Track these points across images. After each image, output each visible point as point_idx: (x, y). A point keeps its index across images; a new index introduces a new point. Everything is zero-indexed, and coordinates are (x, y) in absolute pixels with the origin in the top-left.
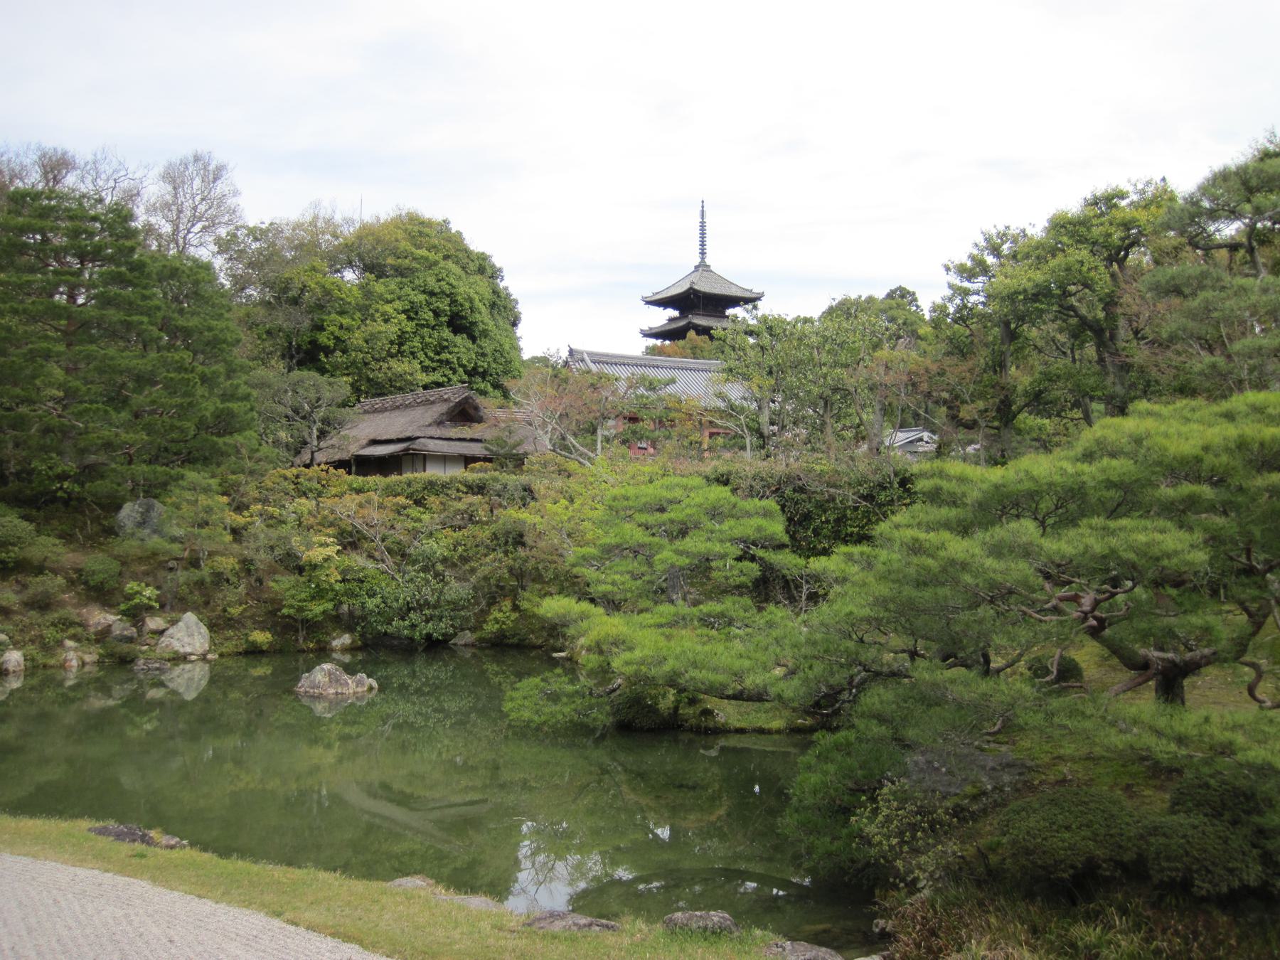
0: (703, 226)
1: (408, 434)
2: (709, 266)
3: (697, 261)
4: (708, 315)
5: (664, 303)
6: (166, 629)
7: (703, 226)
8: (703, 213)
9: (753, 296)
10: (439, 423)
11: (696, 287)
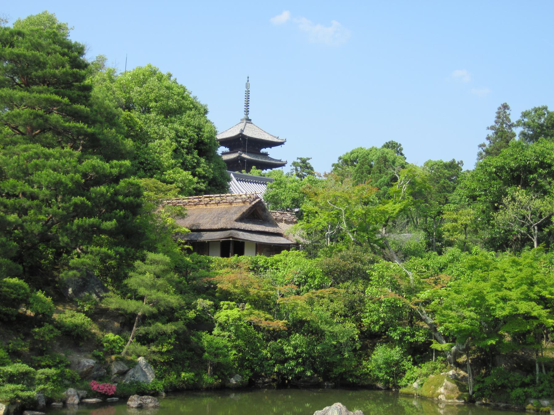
0: (248, 93)
2: (250, 120)
3: (243, 116)
4: (249, 153)
6: (128, 371)
7: (248, 93)
8: (247, 86)
9: (279, 141)
10: (242, 219)
11: (244, 133)
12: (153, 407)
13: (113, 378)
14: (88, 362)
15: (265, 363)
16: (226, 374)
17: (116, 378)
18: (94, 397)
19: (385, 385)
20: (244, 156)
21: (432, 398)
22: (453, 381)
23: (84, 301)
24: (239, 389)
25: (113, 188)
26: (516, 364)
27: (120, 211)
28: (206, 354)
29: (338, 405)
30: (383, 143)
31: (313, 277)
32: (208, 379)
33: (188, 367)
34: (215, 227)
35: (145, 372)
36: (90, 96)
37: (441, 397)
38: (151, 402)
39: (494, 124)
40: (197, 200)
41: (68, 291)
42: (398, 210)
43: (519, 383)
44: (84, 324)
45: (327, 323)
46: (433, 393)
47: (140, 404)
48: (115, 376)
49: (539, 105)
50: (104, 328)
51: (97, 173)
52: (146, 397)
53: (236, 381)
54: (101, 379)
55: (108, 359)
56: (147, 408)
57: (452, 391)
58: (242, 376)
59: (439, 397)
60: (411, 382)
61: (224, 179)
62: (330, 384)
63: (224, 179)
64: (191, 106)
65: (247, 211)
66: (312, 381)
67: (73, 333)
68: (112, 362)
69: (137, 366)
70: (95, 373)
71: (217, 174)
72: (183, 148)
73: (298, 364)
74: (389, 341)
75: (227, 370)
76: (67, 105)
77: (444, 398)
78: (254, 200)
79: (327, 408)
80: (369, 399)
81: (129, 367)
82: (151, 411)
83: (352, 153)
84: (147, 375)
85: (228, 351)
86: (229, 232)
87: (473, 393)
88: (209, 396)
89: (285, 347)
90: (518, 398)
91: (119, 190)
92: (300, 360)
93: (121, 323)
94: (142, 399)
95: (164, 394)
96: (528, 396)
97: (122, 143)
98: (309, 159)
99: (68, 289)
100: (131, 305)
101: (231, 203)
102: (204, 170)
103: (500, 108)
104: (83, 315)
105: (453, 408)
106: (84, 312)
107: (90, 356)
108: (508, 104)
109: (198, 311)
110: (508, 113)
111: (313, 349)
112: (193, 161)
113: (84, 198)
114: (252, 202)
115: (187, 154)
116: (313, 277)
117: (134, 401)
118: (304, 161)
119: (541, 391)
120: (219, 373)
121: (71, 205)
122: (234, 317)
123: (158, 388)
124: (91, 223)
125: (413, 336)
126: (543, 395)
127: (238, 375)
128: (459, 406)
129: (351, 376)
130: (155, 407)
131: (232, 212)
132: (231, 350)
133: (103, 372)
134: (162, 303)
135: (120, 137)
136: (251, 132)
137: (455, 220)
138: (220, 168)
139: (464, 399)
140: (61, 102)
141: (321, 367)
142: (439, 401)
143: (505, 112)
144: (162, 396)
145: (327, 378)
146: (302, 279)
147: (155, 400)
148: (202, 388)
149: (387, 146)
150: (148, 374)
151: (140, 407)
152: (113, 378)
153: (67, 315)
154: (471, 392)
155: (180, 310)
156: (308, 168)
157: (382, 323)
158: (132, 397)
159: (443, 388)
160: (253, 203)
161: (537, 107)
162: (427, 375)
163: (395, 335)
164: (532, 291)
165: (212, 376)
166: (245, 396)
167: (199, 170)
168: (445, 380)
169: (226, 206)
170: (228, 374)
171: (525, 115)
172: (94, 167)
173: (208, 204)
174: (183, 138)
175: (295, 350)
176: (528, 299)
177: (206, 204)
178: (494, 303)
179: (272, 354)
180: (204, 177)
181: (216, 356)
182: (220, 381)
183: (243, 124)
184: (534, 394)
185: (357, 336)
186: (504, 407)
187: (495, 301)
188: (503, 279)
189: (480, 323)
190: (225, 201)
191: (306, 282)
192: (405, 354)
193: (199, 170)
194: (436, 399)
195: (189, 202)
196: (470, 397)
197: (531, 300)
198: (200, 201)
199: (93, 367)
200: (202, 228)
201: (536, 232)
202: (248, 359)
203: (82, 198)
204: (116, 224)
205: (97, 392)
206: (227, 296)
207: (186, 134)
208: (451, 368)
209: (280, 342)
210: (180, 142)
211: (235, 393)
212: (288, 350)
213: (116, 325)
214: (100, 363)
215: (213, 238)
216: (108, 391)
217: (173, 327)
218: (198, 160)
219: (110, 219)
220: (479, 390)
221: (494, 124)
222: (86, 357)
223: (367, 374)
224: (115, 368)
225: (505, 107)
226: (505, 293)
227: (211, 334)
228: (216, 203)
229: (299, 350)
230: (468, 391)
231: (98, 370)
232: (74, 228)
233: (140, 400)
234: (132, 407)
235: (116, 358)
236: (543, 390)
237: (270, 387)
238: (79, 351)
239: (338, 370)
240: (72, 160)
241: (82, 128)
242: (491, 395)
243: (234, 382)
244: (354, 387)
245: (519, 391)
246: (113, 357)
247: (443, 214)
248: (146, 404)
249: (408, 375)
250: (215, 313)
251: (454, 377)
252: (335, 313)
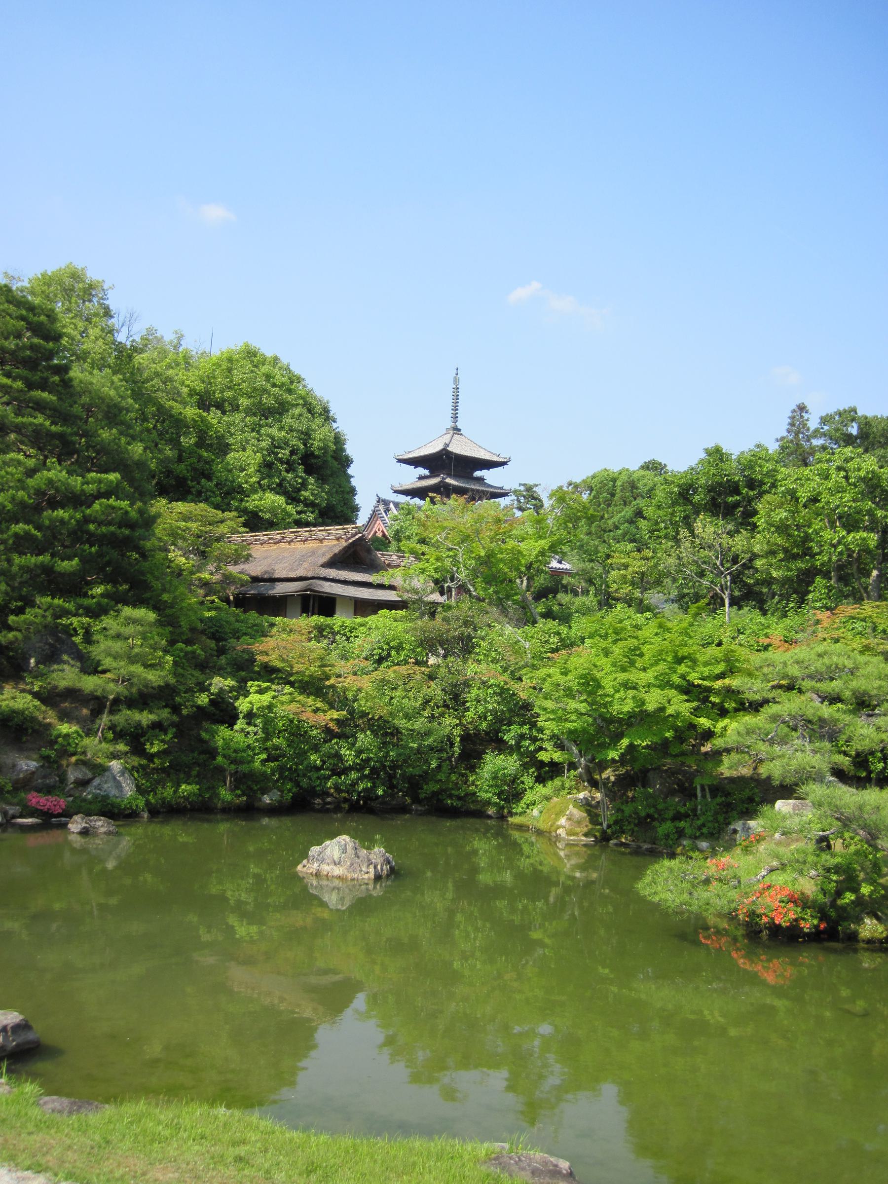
0: (456, 390)
1: (300, 573)
2: (460, 430)
3: (449, 424)
4: (456, 476)
5: (415, 462)
7: (456, 390)
8: (456, 381)
10: (331, 564)
12: (105, 833)
13: (67, 789)
14: (28, 764)
15: (315, 775)
16: (255, 788)
17: (72, 789)
18: (32, 816)
19: (498, 812)
20: (449, 481)
21: (550, 832)
22: (582, 808)
23: (36, 677)
24: (274, 811)
25: (83, 512)
26: (678, 785)
27: (91, 546)
28: (220, 759)
29: (344, 839)
30: (641, 463)
31: (399, 648)
32: (225, 794)
33: (198, 776)
34: (292, 575)
35: (119, 782)
36: (71, 380)
37: (560, 831)
38: (102, 826)
39: (785, 434)
40: (279, 536)
41: (30, 663)
42: (538, 549)
43: (670, 814)
44: (28, 709)
45: (407, 717)
46: (551, 826)
47: (84, 828)
48: (72, 786)
49: (843, 406)
50: (64, 716)
51: (57, 490)
52: (96, 818)
53: (271, 800)
54: (49, 790)
55: (64, 762)
56: (95, 835)
57: (579, 823)
58: (282, 792)
59: (558, 831)
60: (531, 807)
61: (348, 508)
62: (420, 808)
63: (348, 508)
64: (301, 402)
65: (340, 551)
66: (394, 802)
67: (10, 724)
68: (67, 766)
69: (107, 774)
70: (40, 781)
71: (334, 501)
72: (282, 463)
73: (363, 778)
74: (501, 746)
75: (257, 783)
76: (22, 391)
77: (565, 833)
78: (353, 536)
79: (328, 842)
80: (477, 830)
81: (94, 774)
82: (102, 839)
83: (593, 477)
84: (121, 787)
85: (255, 754)
86: (309, 582)
87: (609, 826)
88: (227, 820)
89: (343, 752)
90: (667, 836)
91: (90, 515)
92: (367, 772)
93: (92, 711)
94: (91, 821)
95: (146, 815)
96: (681, 833)
97: (127, 449)
98: (536, 485)
99: (29, 659)
100: (90, 683)
101: (321, 541)
102: (312, 494)
103: (794, 411)
104: (29, 697)
105: (577, 849)
106: (30, 692)
107: (35, 756)
108: (806, 404)
109: (212, 694)
110: (806, 418)
111: (387, 755)
112: (296, 481)
113: (31, 526)
114: (350, 538)
115: (287, 471)
116: (399, 648)
117: (76, 825)
118: (529, 489)
119: (700, 828)
120: (243, 787)
121: (10, 537)
122: (260, 705)
123: (137, 806)
124: (38, 563)
126: (702, 834)
127: (276, 791)
128: (585, 845)
129: (451, 796)
130: (108, 833)
131: (320, 552)
132: (258, 754)
133: (53, 780)
134: (135, 680)
135: (123, 440)
136: (459, 448)
137: (626, 567)
138: (343, 492)
139: (595, 837)
140: (11, 387)
141: (404, 783)
142: (558, 837)
143: (802, 417)
144: (143, 817)
145: (416, 800)
146: (383, 650)
147: (109, 823)
148: (216, 808)
149: (646, 467)
150: (124, 785)
151: (85, 832)
152: (67, 789)
153: (4, 697)
154: (605, 826)
155: (185, 692)
156: (535, 499)
157: (489, 718)
158: (77, 818)
159: (565, 817)
160: (351, 541)
161: (841, 409)
162: (548, 798)
163: (509, 736)
164: (675, 672)
165: (232, 790)
166: (287, 822)
167: (305, 494)
168: (571, 807)
169: (315, 545)
170: (259, 789)
171: (824, 420)
172: (50, 482)
173: (292, 541)
174: (282, 448)
175: (357, 756)
176: (664, 684)
177: (289, 542)
178: (610, 691)
179: (324, 762)
180: (313, 505)
181: (234, 761)
182: (245, 798)
183: (449, 436)
185: (458, 739)
186: (647, 850)
187: (613, 687)
188: (638, 652)
189: (595, 719)
190: (313, 537)
191: (389, 655)
192: (525, 766)
193: (305, 494)
194: (554, 834)
195: (270, 539)
196: (604, 832)
197: (672, 686)
198: (283, 538)
199: (33, 773)
200: (277, 576)
201: (729, 584)
202: (291, 767)
203: (26, 527)
204: (78, 565)
205: (37, 810)
206: (269, 673)
207: (286, 443)
208: (585, 788)
209: (337, 743)
210: (278, 453)
211: (269, 817)
212: (348, 755)
213: (85, 712)
214: (49, 767)
215: (287, 590)
216: (53, 807)
217: (152, 717)
218: (304, 480)
219: (70, 558)
220: (616, 822)
221: (785, 434)
222: (28, 758)
223: (474, 794)
224: (72, 776)
225: (802, 408)
226: (633, 676)
227: (232, 730)
228: (302, 541)
229: (364, 756)
230: (601, 824)
231: (45, 777)
232: (15, 569)
233: (86, 823)
234: (73, 833)
235: (77, 761)
236: (704, 825)
237: (337, 809)
238: (21, 750)
239: (431, 787)
240: (14, 471)
241: (41, 425)
242: (633, 831)
243: (268, 801)
244: (454, 813)
246: (73, 759)
247: (613, 557)
248: (94, 828)
249: (529, 797)
250: (237, 699)
251: (584, 802)
252: (427, 702)
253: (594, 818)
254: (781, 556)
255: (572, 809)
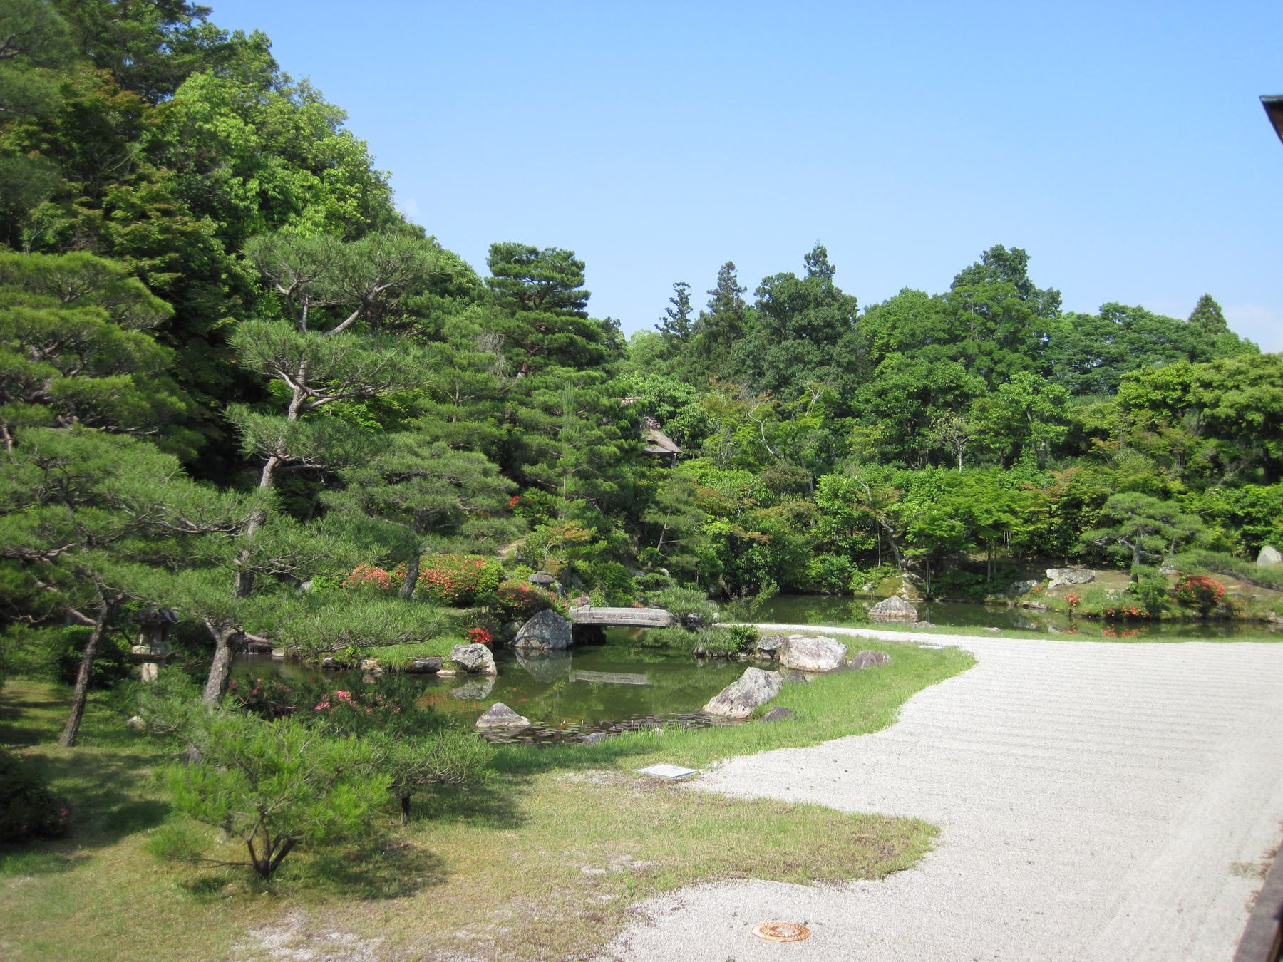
125: (863, 544)
128: (919, 604)
137: (867, 436)
184: (991, 589)
208: (903, 572)
225: (730, 266)
245: (978, 588)
249: (856, 579)
253: (920, 589)
254: (992, 434)
255: (904, 584)
